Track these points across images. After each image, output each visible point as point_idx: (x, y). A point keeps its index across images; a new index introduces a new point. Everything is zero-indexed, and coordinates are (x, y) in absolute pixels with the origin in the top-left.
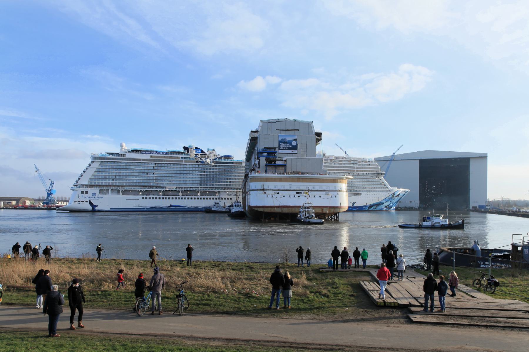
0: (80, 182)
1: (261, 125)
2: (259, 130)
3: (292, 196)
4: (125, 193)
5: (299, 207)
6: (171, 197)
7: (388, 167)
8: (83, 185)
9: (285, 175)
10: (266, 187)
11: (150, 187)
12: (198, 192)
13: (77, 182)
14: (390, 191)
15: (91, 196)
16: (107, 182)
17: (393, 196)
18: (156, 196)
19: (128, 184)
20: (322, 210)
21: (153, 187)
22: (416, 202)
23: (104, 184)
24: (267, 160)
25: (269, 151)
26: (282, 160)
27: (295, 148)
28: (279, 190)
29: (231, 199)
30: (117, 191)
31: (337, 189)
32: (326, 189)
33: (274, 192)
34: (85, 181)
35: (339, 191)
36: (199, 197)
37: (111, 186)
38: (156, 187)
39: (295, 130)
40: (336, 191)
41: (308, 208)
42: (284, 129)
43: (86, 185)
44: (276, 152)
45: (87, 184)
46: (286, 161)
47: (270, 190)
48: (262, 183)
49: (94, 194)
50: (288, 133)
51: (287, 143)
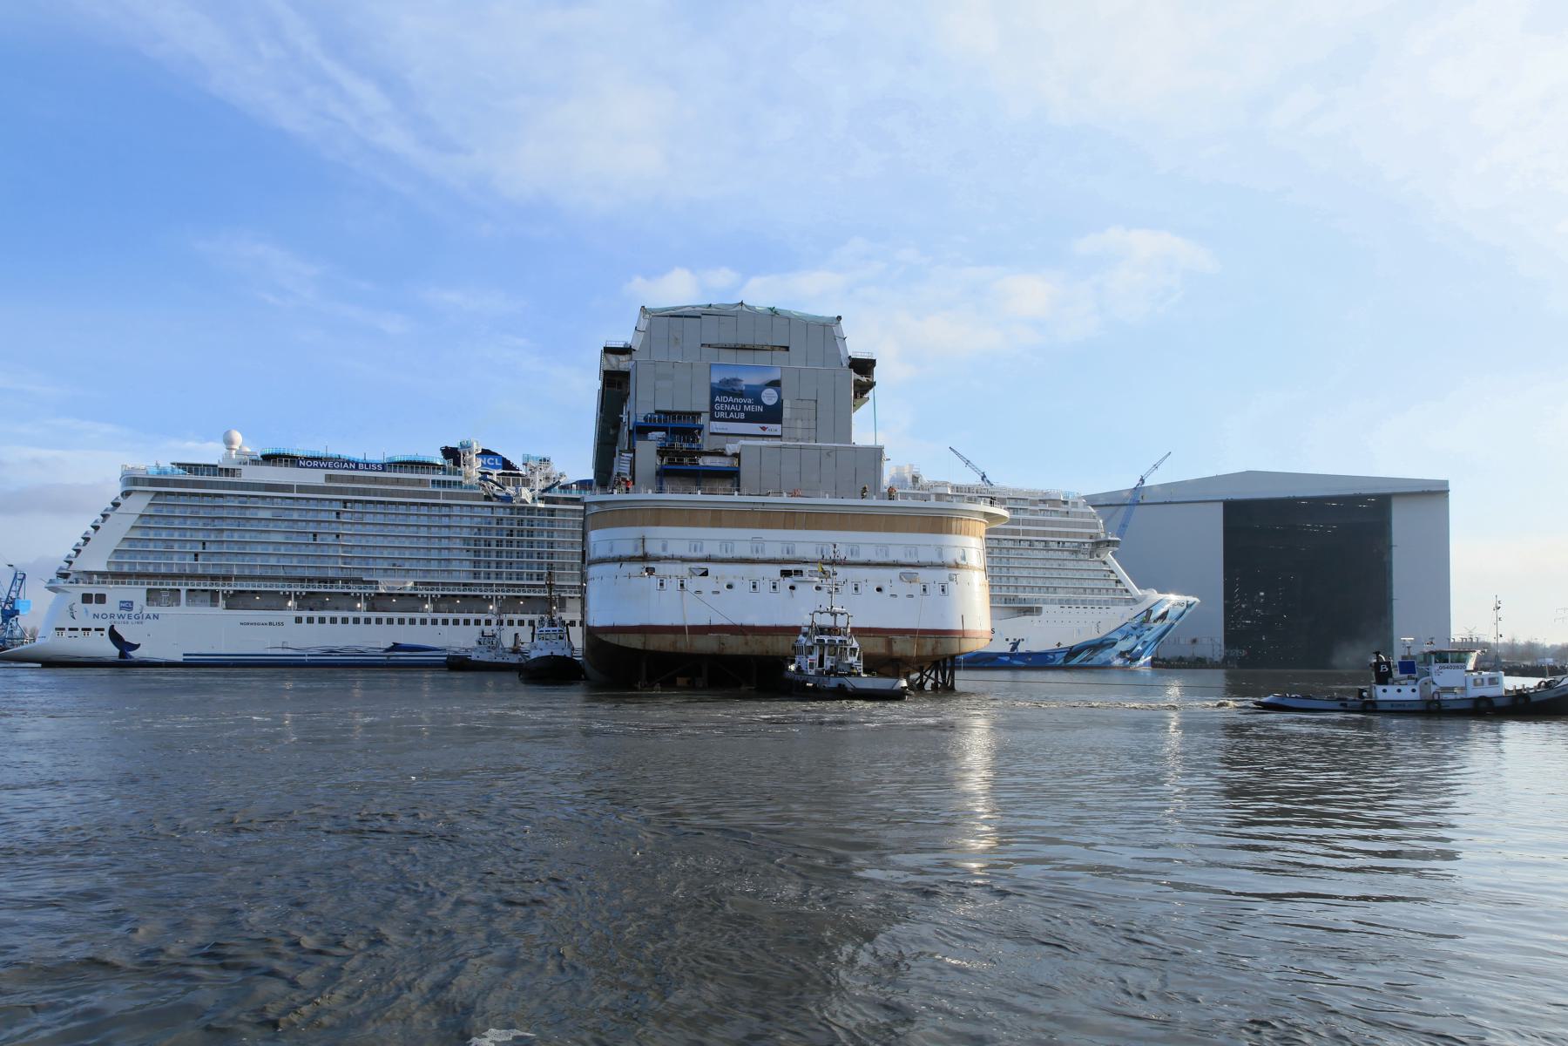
1: (642, 327)
2: (636, 346)
3: (764, 587)
5: (796, 630)
10: (654, 549)
15: (117, 611)
20: (889, 643)
24: (662, 452)
25: (671, 424)
26: (722, 454)
28: (708, 560)
31: (949, 559)
32: (903, 560)
33: (687, 566)
35: (957, 566)
39: (773, 348)
40: (942, 566)
41: (832, 631)
42: (731, 341)
44: (701, 429)
46: (737, 456)
48: (634, 532)
49: (127, 605)
50: (745, 358)
51: (741, 394)
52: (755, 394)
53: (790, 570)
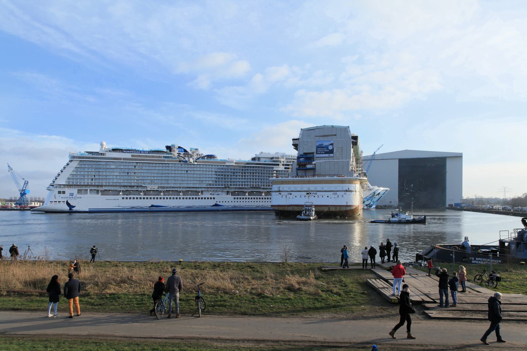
0: (58, 182)
3: (303, 197)
4: (104, 192)
5: (302, 206)
6: (152, 197)
7: (369, 167)
8: (60, 185)
9: (297, 178)
11: (131, 186)
12: (180, 192)
13: (54, 182)
14: (370, 190)
16: (86, 182)
17: (374, 195)
18: (137, 196)
19: (108, 184)
21: (133, 186)
22: (395, 199)
23: (82, 184)
27: (331, 152)
28: (292, 191)
29: (214, 198)
30: (96, 191)
31: (350, 189)
34: (62, 181)
36: (182, 197)
37: (90, 186)
38: (138, 187)
43: (63, 185)
45: (64, 183)
46: (315, 164)
47: (284, 191)
51: (324, 147)
52: (327, 147)
53: (308, 193)
